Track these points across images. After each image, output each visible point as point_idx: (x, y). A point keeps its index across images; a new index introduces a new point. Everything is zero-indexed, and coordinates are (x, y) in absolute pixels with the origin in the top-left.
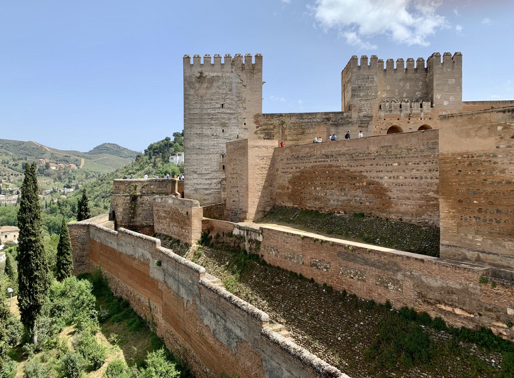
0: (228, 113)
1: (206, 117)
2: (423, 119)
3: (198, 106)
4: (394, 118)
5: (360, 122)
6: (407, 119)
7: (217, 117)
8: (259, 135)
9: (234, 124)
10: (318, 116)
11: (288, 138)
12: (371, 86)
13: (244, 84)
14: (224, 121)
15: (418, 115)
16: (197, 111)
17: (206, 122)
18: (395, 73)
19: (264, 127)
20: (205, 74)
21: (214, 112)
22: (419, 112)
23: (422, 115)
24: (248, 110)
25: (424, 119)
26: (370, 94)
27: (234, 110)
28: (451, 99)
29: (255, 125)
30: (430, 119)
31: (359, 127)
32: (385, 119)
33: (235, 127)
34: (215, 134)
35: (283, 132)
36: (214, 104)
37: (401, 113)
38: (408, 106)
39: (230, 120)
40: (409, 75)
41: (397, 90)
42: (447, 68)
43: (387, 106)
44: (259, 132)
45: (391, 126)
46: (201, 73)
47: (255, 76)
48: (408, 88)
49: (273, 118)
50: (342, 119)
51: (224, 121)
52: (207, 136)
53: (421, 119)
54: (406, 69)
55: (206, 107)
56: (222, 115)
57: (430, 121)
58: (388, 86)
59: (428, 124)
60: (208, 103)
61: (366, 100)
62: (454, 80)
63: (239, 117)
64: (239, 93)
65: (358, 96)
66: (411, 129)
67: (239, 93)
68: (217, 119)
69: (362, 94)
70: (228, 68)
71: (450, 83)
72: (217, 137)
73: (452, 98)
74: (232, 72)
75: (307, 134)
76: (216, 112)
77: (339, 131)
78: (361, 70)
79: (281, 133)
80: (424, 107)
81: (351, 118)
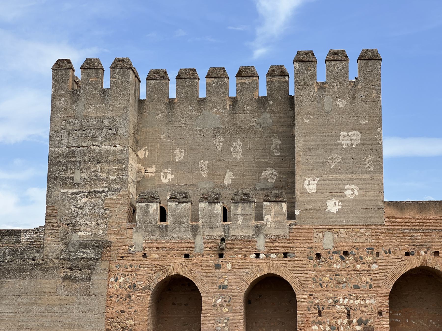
2: (262, 256)
4: (172, 253)
5: (69, 264)
6: (214, 257)
12: (107, 152)
22: (250, 233)
23: (261, 244)
25: (268, 255)
26: (103, 176)
28: (348, 193)
30: (285, 255)
31: (65, 278)
32: (145, 256)
37: (195, 236)
38: (217, 215)
40: (242, 116)
41: (204, 164)
42: (335, 97)
43: (153, 215)
45: (163, 277)
48: (239, 156)
50: (14, 252)
53: (258, 255)
54: (234, 100)
57: (283, 262)
58: (177, 151)
59: (279, 274)
61: (90, 195)
66: (224, 287)
71: (345, 143)
78: (80, 105)
81: (40, 250)
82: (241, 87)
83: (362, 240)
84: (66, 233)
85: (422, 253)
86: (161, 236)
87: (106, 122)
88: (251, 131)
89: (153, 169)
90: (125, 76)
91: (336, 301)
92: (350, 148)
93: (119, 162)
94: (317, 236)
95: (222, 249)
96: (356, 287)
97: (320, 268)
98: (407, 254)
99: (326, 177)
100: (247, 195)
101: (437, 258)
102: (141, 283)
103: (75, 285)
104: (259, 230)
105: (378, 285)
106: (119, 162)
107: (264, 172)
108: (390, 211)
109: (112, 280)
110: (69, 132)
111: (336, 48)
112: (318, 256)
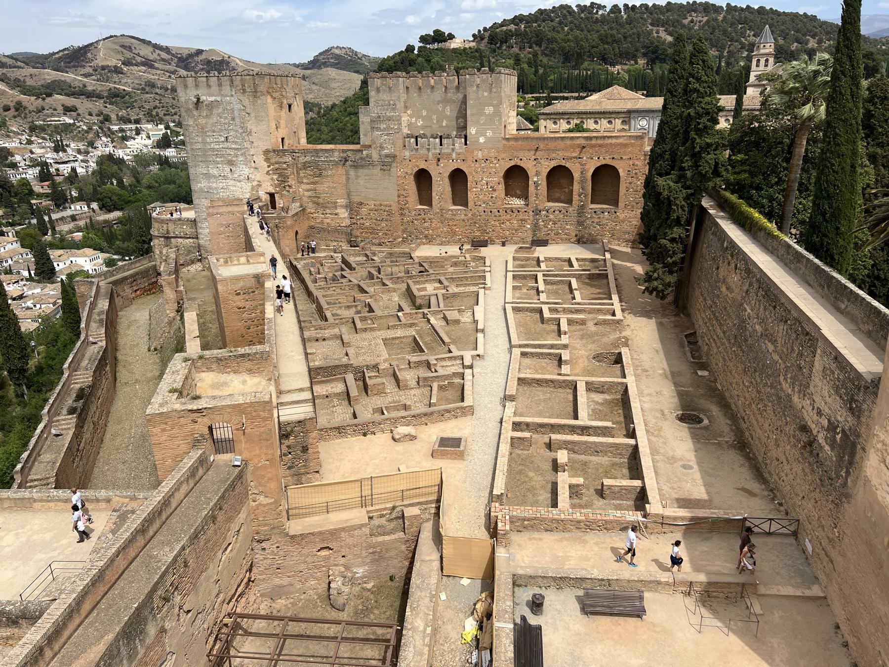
0: (234, 149)
1: (210, 153)
8: (271, 176)
13: (248, 110)
18: (432, 92)
19: (277, 166)
20: (203, 98)
21: (218, 146)
22: (450, 151)
23: (454, 156)
24: (255, 144)
27: (240, 145)
28: (488, 134)
29: (265, 164)
33: (244, 166)
35: (298, 173)
40: (449, 95)
41: (434, 117)
42: (483, 91)
44: (271, 172)
46: (198, 99)
47: (259, 102)
48: (448, 113)
49: (285, 156)
50: (361, 158)
52: (215, 177)
56: (228, 151)
61: (388, 135)
62: (491, 108)
64: (243, 123)
65: (378, 129)
67: (243, 123)
68: (222, 156)
69: (383, 126)
73: (489, 133)
74: (232, 96)
76: (221, 146)
78: (381, 95)
81: (371, 158)
88: (454, 102)
90: (398, 81)
92: (489, 114)
93: (398, 120)
102: (409, 172)
104: (453, 150)
106: (398, 120)
108: (504, 142)
110: (377, 106)
112: (476, 161)
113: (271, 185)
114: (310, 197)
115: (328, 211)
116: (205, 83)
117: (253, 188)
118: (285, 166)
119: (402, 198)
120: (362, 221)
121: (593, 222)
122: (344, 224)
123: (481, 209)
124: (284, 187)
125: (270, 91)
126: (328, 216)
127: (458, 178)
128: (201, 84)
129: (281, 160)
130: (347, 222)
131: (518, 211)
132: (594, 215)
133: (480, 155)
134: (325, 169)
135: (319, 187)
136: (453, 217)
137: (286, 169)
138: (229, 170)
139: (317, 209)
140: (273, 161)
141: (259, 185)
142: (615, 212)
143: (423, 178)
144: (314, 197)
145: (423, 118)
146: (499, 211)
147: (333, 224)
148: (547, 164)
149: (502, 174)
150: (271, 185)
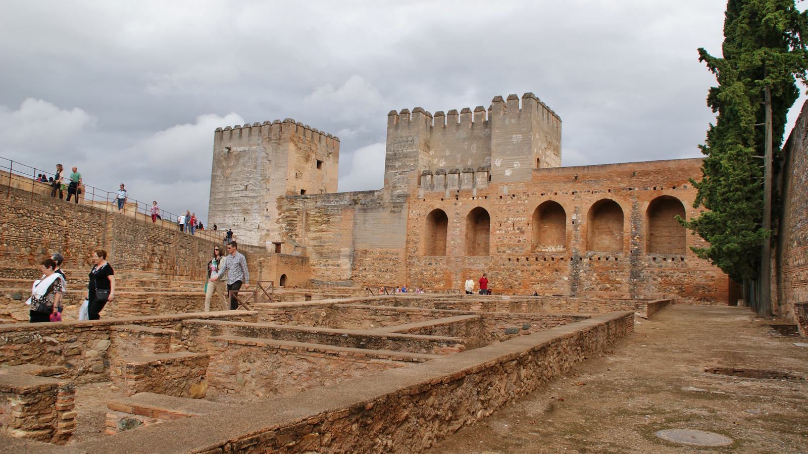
1: (230, 202)
2: (475, 198)
3: (223, 189)
5: (393, 205)
6: (455, 199)
7: (240, 201)
8: (280, 224)
9: (255, 211)
10: (347, 197)
11: (312, 228)
14: (246, 206)
15: (469, 192)
16: (221, 196)
17: (229, 209)
18: (457, 130)
19: (287, 214)
20: (233, 149)
21: (237, 195)
22: (470, 187)
23: (475, 193)
24: (270, 192)
25: (478, 197)
26: (408, 164)
28: (515, 165)
29: (277, 212)
30: (486, 197)
31: (391, 212)
34: (236, 224)
36: (238, 186)
39: (252, 205)
40: (476, 131)
41: (459, 156)
42: (511, 118)
44: (281, 220)
46: (229, 149)
47: (281, 148)
48: (474, 151)
50: (372, 201)
51: (246, 206)
53: (473, 198)
54: (473, 124)
55: (230, 189)
56: (245, 199)
58: (447, 151)
60: (232, 185)
62: (520, 136)
63: (262, 201)
64: (263, 170)
65: (393, 167)
66: (458, 214)
67: (263, 170)
68: (240, 205)
69: (397, 164)
70: (255, 138)
71: (515, 141)
72: (238, 227)
73: (517, 165)
74: (258, 144)
75: (332, 222)
76: (240, 195)
77: (367, 218)
78: (399, 131)
79: (304, 222)
80: (479, 180)
81: (382, 200)
82: (476, 117)
83: (521, 189)
84: (392, 191)
85: (549, 194)
86: (432, 190)
87: (410, 139)
89: (437, 160)
91: (508, 219)
93: (415, 157)
94: (500, 187)
95: (457, 196)
96: (517, 212)
97: (501, 203)
98: (542, 195)
99: (505, 158)
100: (469, 169)
101: (556, 196)
103: (395, 215)
105: (527, 211)
106: (415, 157)
107: (486, 158)
108: (535, 173)
109: (410, 212)
111: (512, 93)
112: (501, 197)
113: (279, 234)
114: (315, 246)
115: (330, 262)
116: (238, 135)
117: (261, 239)
118: (295, 213)
119: (411, 245)
120: (364, 273)
121: (651, 272)
122: (345, 277)
123: (505, 256)
124: (291, 237)
125: (295, 139)
126: (330, 267)
127: (480, 217)
128: (234, 136)
129: (293, 207)
130: (348, 274)
131: (553, 259)
132: (653, 263)
133: (505, 190)
134: (334, 215)
135: (325, 235)
136: (471, 267)
137: (295, 217)
138: (243, 219)
139: (320, 260)
140: (284, 208)
141: (268, 235)
142: (682, 259)
143: (439, 218)
144: (320, 246)
145: (446, 158)
146: (527, 259)
147: (334, 277)
148: (588, 197)
149: (532, 212)
150: (279, 234)
